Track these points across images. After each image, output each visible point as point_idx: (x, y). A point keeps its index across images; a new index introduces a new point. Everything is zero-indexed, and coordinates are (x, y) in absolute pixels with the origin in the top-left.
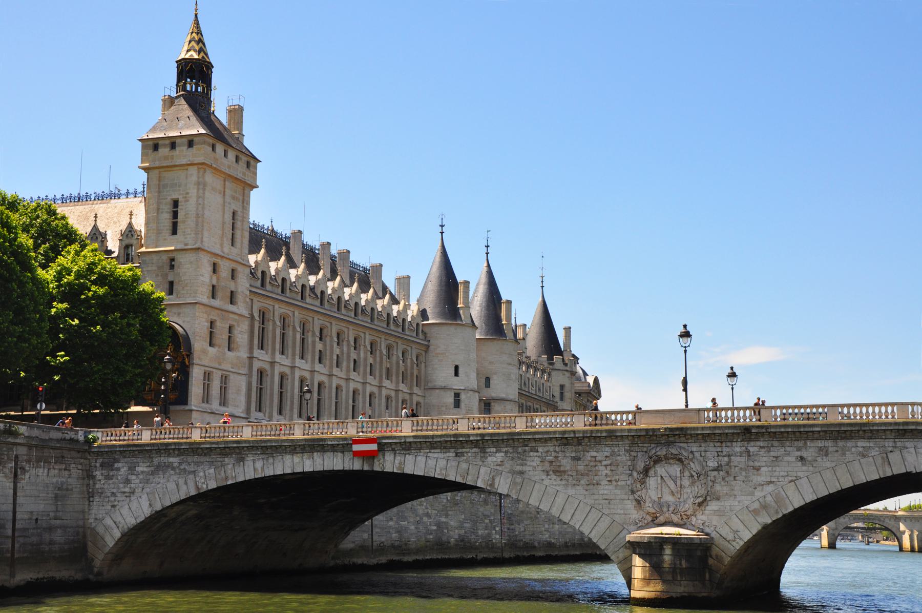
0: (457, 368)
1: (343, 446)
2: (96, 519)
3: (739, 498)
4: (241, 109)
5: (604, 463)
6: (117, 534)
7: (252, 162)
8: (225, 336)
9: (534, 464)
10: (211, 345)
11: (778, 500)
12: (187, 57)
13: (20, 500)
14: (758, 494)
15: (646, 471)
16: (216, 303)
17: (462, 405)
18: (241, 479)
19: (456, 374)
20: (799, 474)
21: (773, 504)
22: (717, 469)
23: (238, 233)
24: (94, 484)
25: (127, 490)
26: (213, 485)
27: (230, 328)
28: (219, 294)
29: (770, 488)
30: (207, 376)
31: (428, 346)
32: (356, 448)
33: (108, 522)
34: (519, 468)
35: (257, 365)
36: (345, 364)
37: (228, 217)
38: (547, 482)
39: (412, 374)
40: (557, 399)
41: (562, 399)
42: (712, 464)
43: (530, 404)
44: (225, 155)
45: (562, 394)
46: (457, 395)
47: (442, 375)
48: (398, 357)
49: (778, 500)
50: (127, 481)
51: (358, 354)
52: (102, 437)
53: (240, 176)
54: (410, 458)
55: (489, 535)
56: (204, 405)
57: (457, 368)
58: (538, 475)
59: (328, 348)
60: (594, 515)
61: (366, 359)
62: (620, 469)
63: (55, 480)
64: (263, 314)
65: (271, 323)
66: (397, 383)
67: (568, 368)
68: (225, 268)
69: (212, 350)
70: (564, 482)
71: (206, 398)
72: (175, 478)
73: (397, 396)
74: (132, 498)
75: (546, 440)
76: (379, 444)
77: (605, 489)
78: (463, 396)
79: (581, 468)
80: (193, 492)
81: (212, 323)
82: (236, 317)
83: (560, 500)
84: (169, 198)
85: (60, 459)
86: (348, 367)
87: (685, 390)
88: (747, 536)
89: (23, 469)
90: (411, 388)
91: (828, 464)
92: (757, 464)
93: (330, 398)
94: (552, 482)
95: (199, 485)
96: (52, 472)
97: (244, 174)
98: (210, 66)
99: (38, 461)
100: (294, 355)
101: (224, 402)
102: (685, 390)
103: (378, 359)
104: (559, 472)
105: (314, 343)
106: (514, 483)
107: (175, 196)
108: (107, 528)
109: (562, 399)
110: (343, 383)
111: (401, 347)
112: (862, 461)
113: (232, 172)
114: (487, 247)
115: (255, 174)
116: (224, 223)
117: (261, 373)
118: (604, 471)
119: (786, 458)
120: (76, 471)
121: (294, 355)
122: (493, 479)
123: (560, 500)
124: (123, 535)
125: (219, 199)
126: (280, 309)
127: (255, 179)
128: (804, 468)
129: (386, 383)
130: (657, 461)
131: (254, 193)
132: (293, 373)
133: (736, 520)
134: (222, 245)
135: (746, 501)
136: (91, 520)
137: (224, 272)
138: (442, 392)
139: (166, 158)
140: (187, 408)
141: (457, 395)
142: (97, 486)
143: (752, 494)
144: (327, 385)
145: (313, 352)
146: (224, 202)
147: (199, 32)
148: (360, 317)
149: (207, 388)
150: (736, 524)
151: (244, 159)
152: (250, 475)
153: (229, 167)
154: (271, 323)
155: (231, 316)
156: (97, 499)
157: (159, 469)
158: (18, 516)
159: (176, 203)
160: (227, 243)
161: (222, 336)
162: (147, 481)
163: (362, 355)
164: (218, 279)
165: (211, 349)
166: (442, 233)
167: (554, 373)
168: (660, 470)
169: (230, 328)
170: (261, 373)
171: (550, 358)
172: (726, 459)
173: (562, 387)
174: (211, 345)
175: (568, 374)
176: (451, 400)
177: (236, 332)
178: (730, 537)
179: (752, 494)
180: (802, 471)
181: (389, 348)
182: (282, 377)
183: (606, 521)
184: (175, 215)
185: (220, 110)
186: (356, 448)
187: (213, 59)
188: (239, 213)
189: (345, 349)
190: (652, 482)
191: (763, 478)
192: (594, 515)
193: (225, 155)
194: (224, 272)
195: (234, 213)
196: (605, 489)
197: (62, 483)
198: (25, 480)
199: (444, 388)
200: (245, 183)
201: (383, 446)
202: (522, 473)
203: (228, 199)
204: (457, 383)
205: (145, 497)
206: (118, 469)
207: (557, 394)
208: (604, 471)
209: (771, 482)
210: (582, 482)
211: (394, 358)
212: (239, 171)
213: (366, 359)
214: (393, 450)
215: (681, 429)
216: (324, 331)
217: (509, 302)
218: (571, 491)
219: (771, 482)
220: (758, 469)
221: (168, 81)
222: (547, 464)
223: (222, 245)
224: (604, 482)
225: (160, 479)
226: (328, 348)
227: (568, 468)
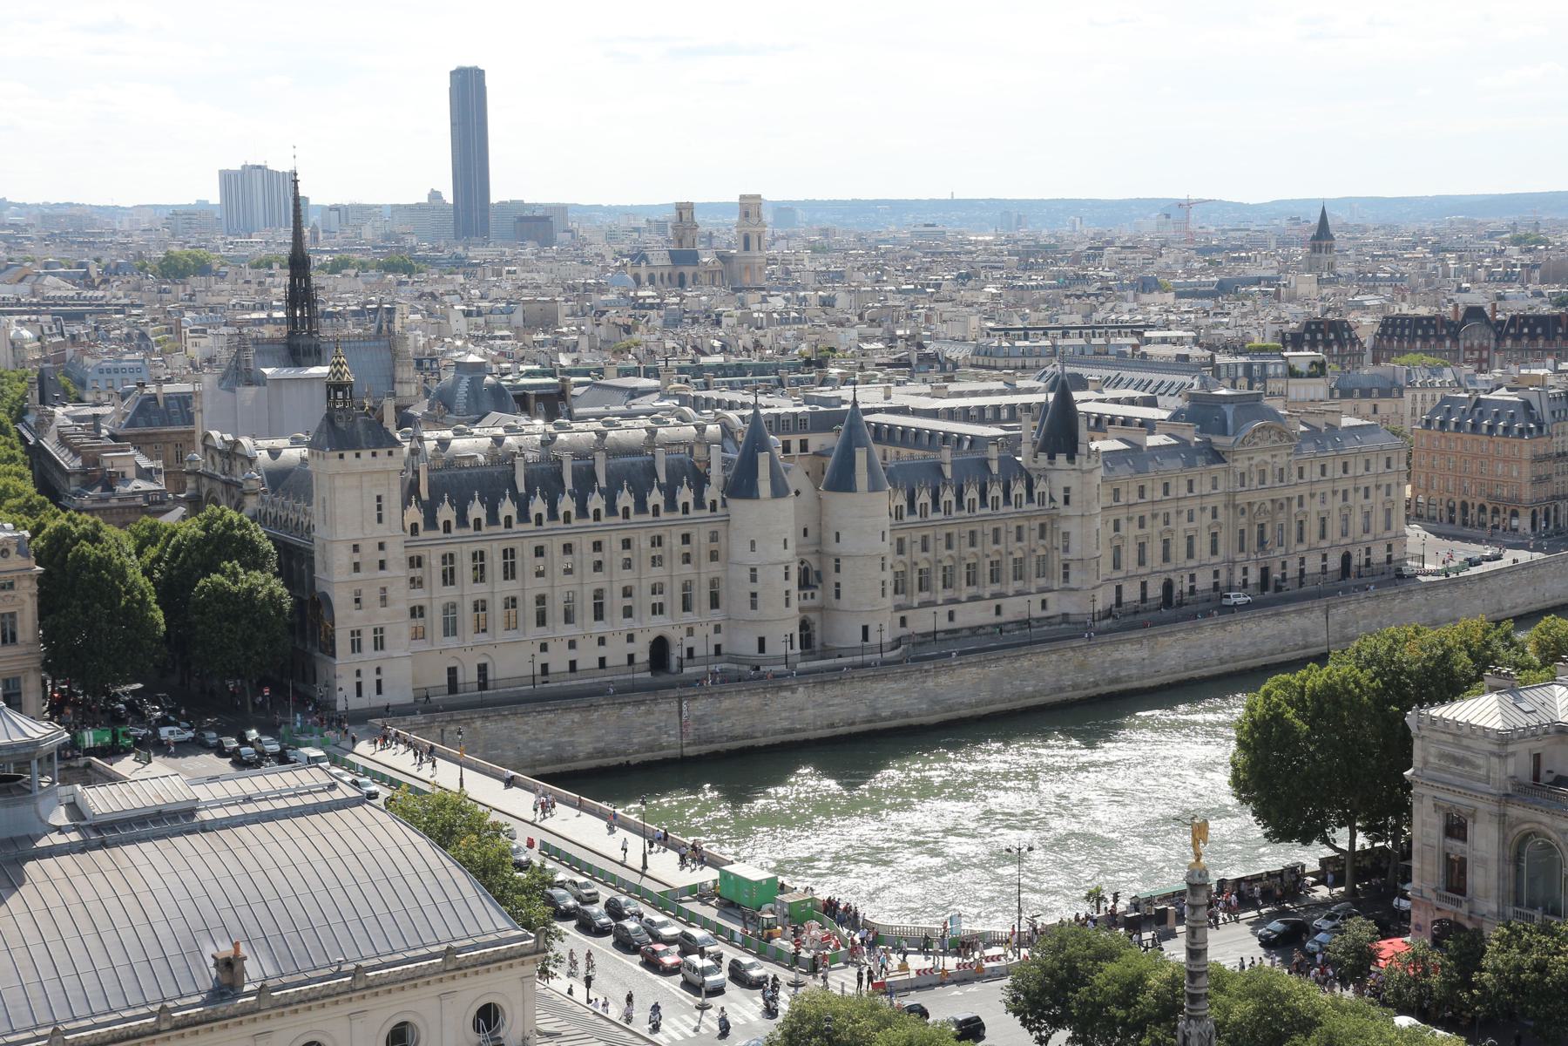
0: (753, 543)
23: (385, 512)
28: (362, 567)
41: (1067, 501)
44: (358, 455)
46: (754, 570)
47: (740, 550)
57: (753, 543)
68: (369, 549)
109: (1067, 501)
171: (1052, 457)
173: (1067, 490)
176: (747, 575)
193: (358, 455)
195: (379, 498)
204: (753, 559)
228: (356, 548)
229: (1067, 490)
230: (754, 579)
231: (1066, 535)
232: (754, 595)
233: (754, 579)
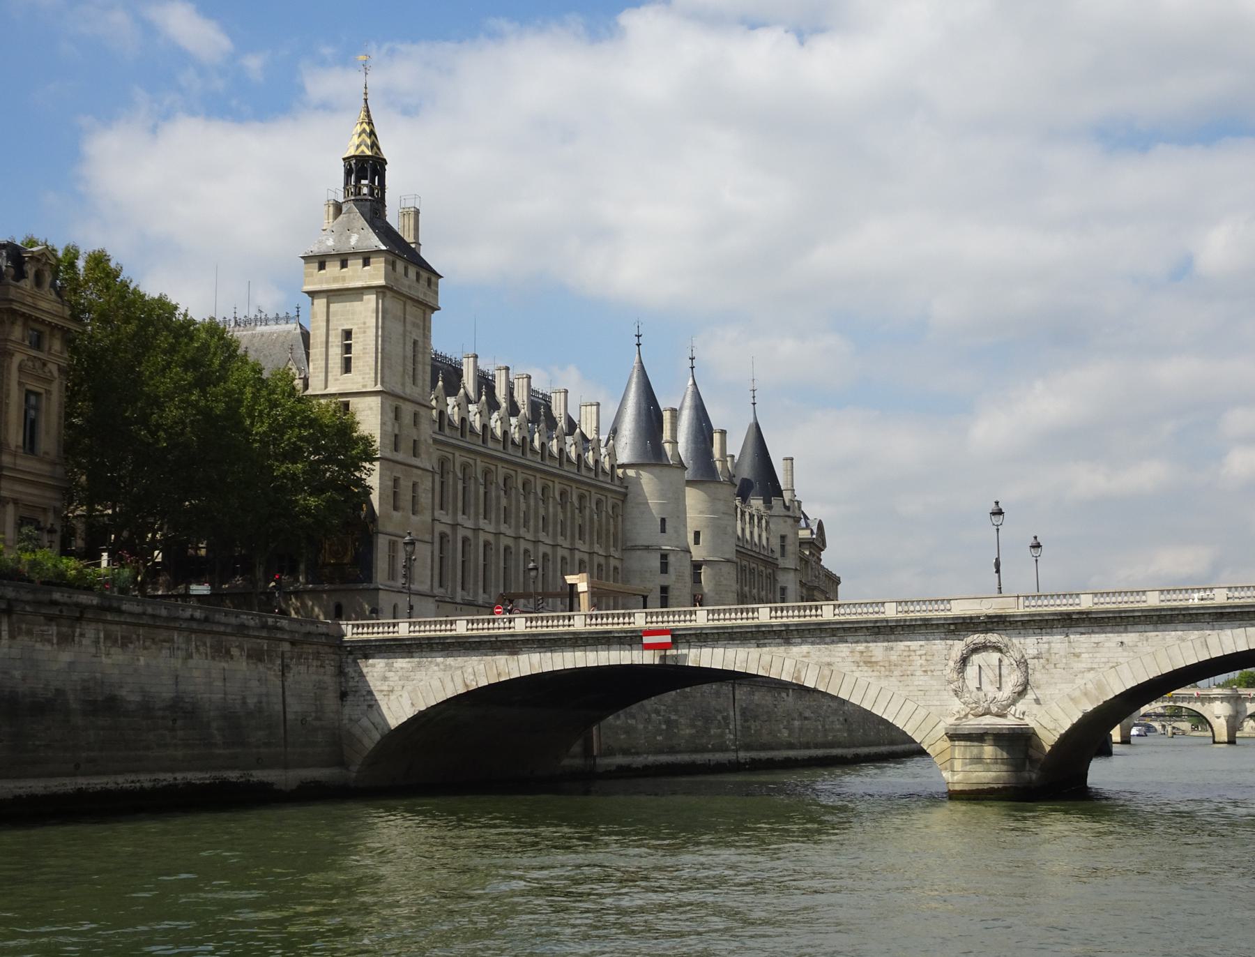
1: (632, 639)
2: (350, 720)
3: (1059, 686)
4: (417, 212)
5: (918, 653)
6: (377, 736)
7: (433, 279)
8: (409, 497)
9: (843, 655)
10: (396, 508)
11: (1100, 687)
12: (357, 153)
13: (289, 700)
14: (1079, 681)
15: (964, 661)
16: (400, 456)
17: (671, 569)
18: (515, 675)
19: (663, 530)
20: (1120, 660)
21: (1094, 691)
22: (1037, 657)
23: (420, 367)
24: (347, 681)
25: (385, 688)
26: (483, 682)
27: (415, 485)
28: (402, 446)
29: (1091, 675)
30: (393, 546)
31: (626, 495)
32: (646, 640)
33: (365, 722)
34: (828, 660)
35: (439, 528)
36: (532, 523)
37: (410, 353)
38: (857, 674)
39: (608, 531)
40: (777, 555)
41: (783, 555)
42: (1032, 651)
43: (744, 563)
44: (406, 274)
45: (783, 547)
46: (664, 557)
47: (646, 532)
48: (592, 510)
49: (1100, 687)
50: (385, 679)
51: (547, 509)
52: (350, 631)
53: (421, 296)
54: (706, 651)
55: (722, 735)
56: (389, 583)
58: (847, 667)
59: (514, 502)
60: (910, 706)
61: (555, 515)
62: (936, 658)
63: (314, 677)
64: (443, 462)
65: (451, 475)
66: (592, 544)
67: (790, 513)
69: (397, 515)
70: (875, 674)
71: (392, 575)
72: (440, 674)
73: (591, 560)
74: (392, 697)
75: (856, 629)
76: (673, 636)
77: (920, 680)
78: (671, 559)
79: (894, 658)
80: (462, 690)
81: (396, 480)
82: (420, 472)
83: (872, 693)
84: (340, 328)
85: (317, 655)
86: (536, 526)
87: (998, 571)
88: (1066, 725)
89: (288, 666)
90: (607, 548)
91: (1149, 649)
92: (1077, 651)
93: (517, 566)
94: (864, 675)
95: (468, 682)
96: (312, 669)
97: (425, 294)
98: (384, 162)
99: (300, 657)
100: (477, 515)
101: (408, 576)
102: (998, 571)
103: (569, 514)
104: (869, 663)
105: (498, 498)
106: (820, 677)
107: (347, 327)
108: (365, 730)
109: (783, 555)
110: (530, 547)
111: (595, 497)
112: (1183, 644)
113: (413, 293)
114: (692, 359)
115: (437, 293)
116: (405, 357)
117: (443, 536)
118: (919, 662)
119: (1106, 644)
120: (330, 669)
121: (477, 515)
122: (799, 671)
123: (872, 693)
124: (383, 738)
125: (400, 328)
126: (459, 458)
127: (437, 300)
128: (1125, 654)
129: (579, 544)
130: (976, 649)
131: (435, 316)
132: (477, 537)
133: (1057, 708)
134: (403, 385)
135: (1067, 688)
136: (345, 722)
137: (407, 418)
138: (645, 554)
139: (335, 280)
140: (372, 586)
141: (664, 557)
142: (351, 684)
143: (1073, 682)
144: (513, 550)
145: (498, 509)
146: (405, 331)
147: (370, 123)
148: (547, 462)
149: (392, 559)
150: (1059, 714)
151: (424, 275)
152: (526, 672)
153: (410, 287)
154: (451, 475)
155: (415, 471)
156: (350, 698)
157: (419, 665)
158: (289, 716)
159: (348, 334)
160: (409, 381)
161: (406, 497)
162: (407, 678)
163: (551, 509)
164: (400, 427)
165: (395, 513)
166: (639, 345)
167: (772, 520)
168: (976, 659)
169: (415, 485)
170: (443, 536)
171: (767, 503)
172: (1046, 646)
173: (783, 538)
174: (396, 508)
175: (790, 521)
176: (656, 563)
177: (420, 490)
178: (1051, 726)
179: (1073, 682)
180: (1121, 656)
181: (581, 497)
182: (465, 540)
183: (922, 712)
184: (348, 349)
185: (392, 217)
186: (646, 640)
187: (386, 154)
188: (420, 344)
189: (532, 503)
190: (971, 671)
191: (1084, 665)
192: (910, 706)
194: (407, 418)
195: (415, 343)
196: (920, 680)
197: (320, 681)
198: (290, 677)
199: (647, 548)
200: (426, 305)
201: (679, 638)
202: (829, 664)
203: (409, 327)
205: (405, 695)
206: (373, 666)
207: (777, 548)
208: (919, 662)
209: (1092, 669)
210: (896, 673)
211: (587, 512)
212: (420, 292)
213: (555, 515)
214: (688, 642)
215: (1001, 616)
216: (508, 482)
217: (723, 433)
218: (884, 683)
219: (1092, 669)
220: (1077, 655)
221: (334, 182)
222: (858, 655)
223: (403, 385)
224: (918, 673)
225: (420, 674)
226: (514, 502)
227: (880, 658)
228: (397, 411)
229: (783, 538)
230: (664, 568)
231: (783, 590)
232: (664, 589)
233: (664, 568)
